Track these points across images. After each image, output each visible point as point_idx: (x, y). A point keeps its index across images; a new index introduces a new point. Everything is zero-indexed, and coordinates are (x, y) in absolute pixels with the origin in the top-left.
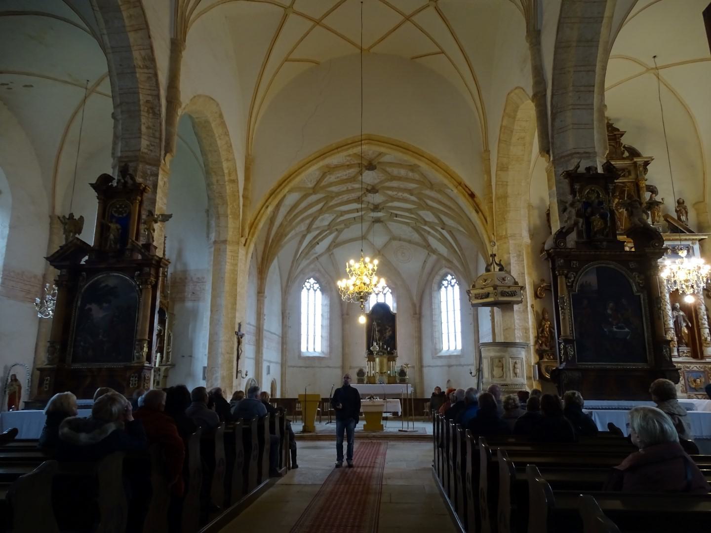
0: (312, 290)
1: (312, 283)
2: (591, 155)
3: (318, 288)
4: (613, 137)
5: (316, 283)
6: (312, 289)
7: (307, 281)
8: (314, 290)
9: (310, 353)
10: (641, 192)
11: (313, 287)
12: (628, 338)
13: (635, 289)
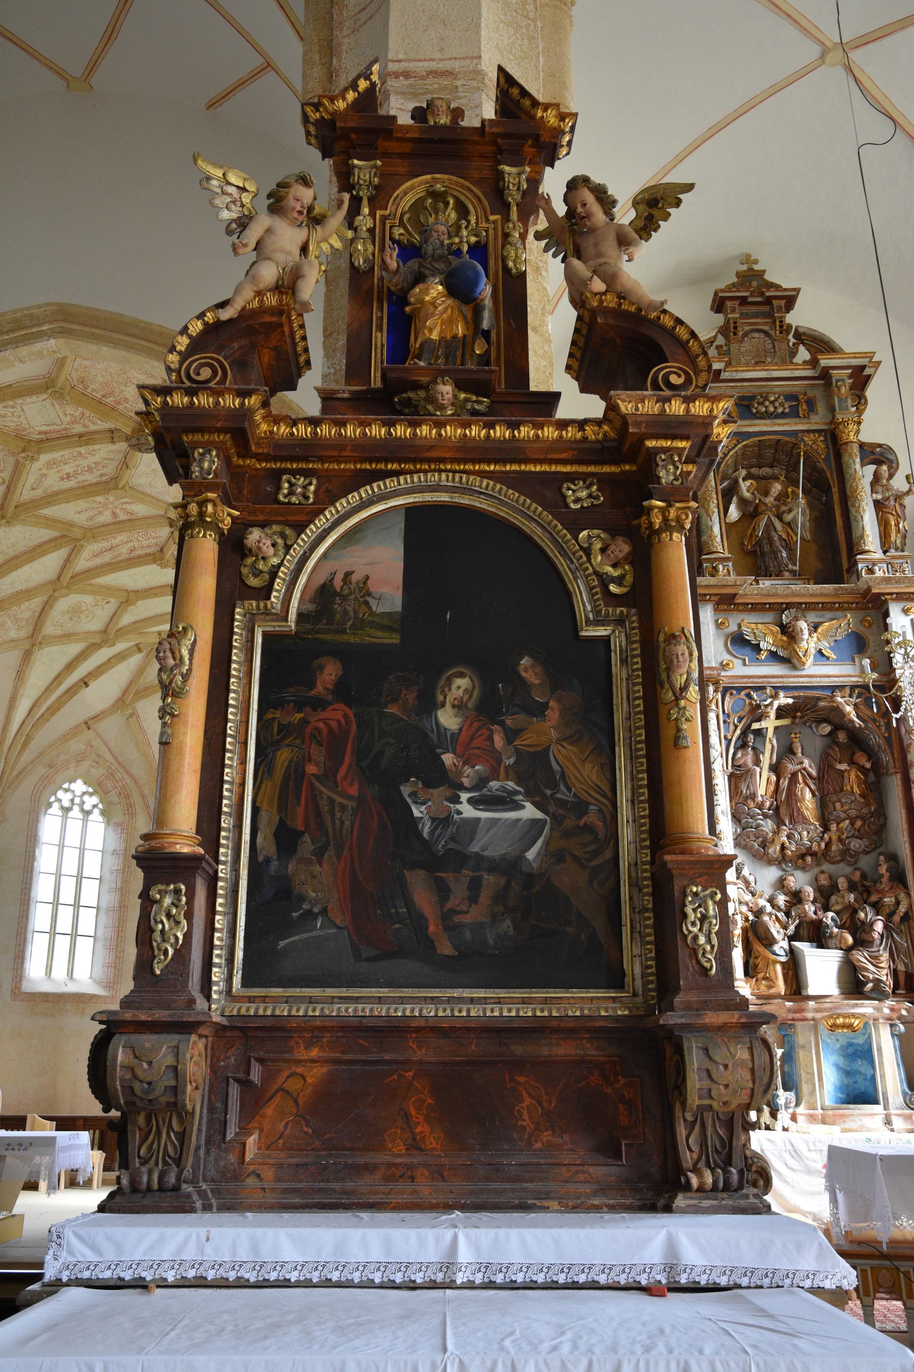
0: (76, 812)
1: (78, 793)
2: (459, 83)
3: (95, 806)
4: (766, 308)
5: (91, 794)
6: (76, 808)
7: (66, 786)
8: (82, 810)
9: (54, 981)
10: (846, 458)
11: (83, 803)
12: (531, 855)
13: (583, 604)
